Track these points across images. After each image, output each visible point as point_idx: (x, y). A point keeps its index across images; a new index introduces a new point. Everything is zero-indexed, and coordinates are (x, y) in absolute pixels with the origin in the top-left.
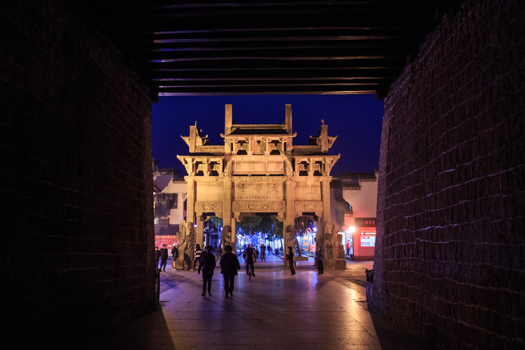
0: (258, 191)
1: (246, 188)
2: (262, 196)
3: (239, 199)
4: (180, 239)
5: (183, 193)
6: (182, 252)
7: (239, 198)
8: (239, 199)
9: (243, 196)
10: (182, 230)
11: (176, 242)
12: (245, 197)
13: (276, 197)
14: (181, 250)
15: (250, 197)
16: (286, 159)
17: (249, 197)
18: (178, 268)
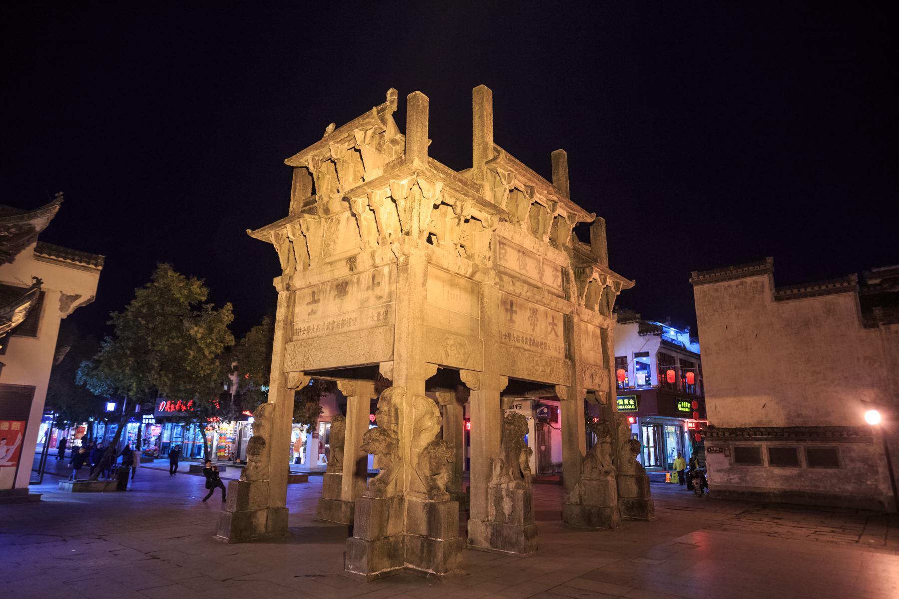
0: (532, 327)
1: (516, 312)
2: (539, 340)
3: (505, 338)
4: (393, 456)
5: (63, 295)
6: (394, 506)
7: (505, 335)
8: (505, 338)
9: (512, 334)
10: (393, 421)
11: (7, 444)
12: (516, 336)
13: (556, 348)
14: (392, 499)
15: (522, 337)
16: (568, 264)
17: (521, 340)
18: (385, 570)
